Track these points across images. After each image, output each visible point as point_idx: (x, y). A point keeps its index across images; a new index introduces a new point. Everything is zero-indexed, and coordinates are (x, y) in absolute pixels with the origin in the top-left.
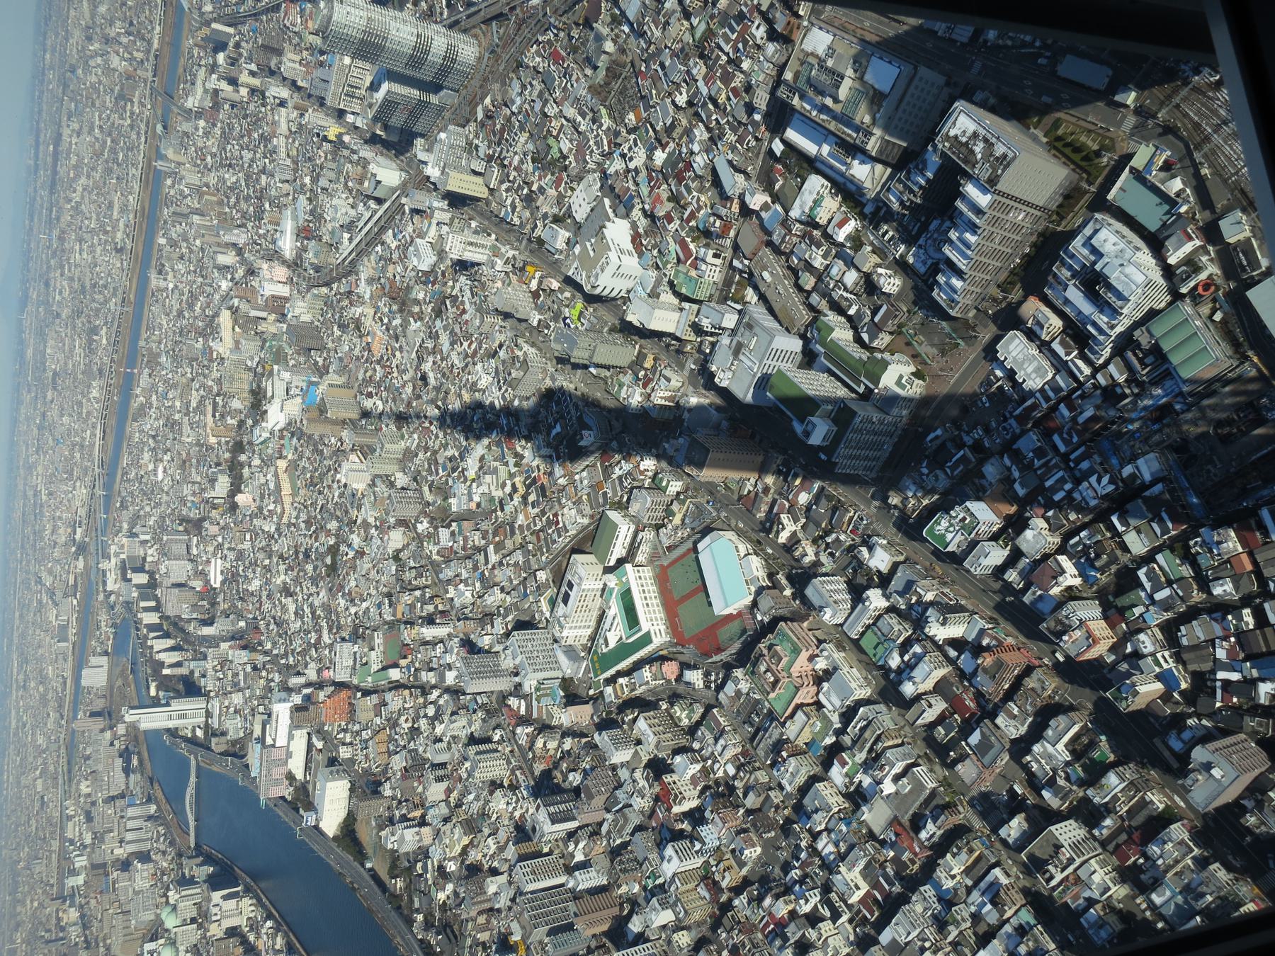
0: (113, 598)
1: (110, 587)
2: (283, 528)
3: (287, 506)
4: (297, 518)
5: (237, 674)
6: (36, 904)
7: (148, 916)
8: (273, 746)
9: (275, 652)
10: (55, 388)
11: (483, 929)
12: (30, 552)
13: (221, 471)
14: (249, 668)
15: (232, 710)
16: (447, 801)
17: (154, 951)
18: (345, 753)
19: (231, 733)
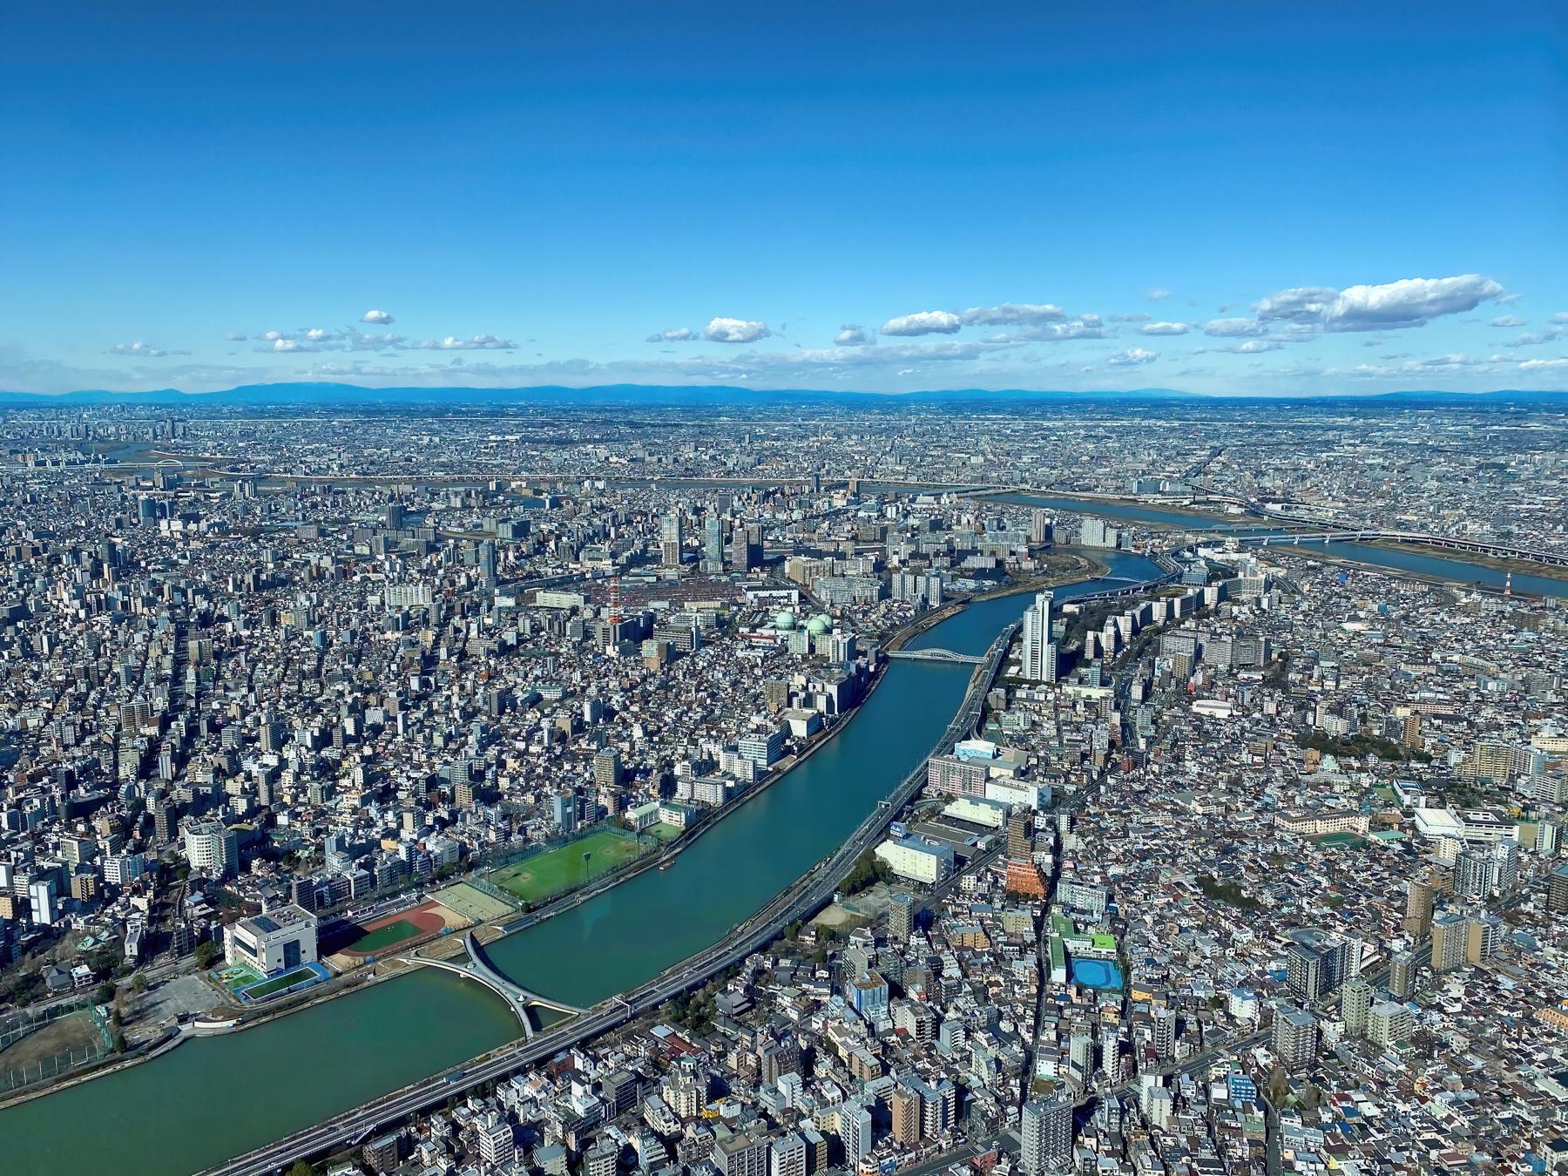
0: (1188, 555)
1: (1202, 552)
2: (1267, 818)
3: (1298, 827)
4: (1282, 841)
5: (1078, 730)
6: (857, 457)
7: (824, 596)
8: (988, 779)
9: (1103, 789)
10: (1480, 467)
11: (741, 1061)
12: (1253, 439)
13: (1353, 728)
14: (1085, 747)
15: (1036, 718)
16: (893, 1031)
17: (790, 600)
18: (968, 882)
19: (1008, 717)
